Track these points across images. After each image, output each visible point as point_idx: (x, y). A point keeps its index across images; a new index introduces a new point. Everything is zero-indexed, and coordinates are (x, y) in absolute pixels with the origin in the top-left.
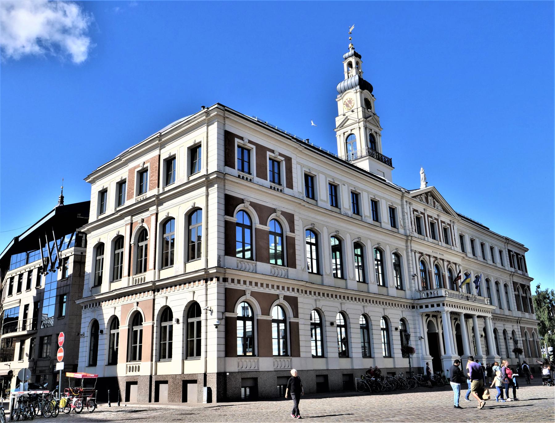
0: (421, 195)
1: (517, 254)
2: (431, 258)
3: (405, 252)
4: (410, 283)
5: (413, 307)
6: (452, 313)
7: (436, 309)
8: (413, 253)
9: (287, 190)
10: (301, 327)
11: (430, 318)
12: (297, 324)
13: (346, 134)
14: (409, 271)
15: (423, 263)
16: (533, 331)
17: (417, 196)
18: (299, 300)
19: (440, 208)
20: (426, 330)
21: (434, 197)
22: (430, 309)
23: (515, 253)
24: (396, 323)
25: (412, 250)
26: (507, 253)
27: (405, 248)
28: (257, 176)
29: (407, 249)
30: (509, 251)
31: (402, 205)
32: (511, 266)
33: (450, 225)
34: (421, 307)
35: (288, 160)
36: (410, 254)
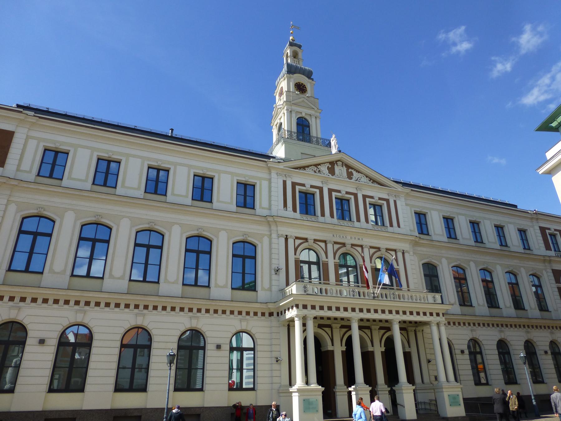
0: (319, 164)
2: (330, 246)
3: (266, 240)
4: (271, 280)
5: (271, 314)
8: (283, 240)
14: (271, 264)
17: (308, 166)
19: (364, 179)
25: (279, 236)
26: (539, 231)
27: (268, 233)
29: (270, 236)
30: (543, 230)
31: (270, 181)
33: (388, 201)
36: (274, 241)
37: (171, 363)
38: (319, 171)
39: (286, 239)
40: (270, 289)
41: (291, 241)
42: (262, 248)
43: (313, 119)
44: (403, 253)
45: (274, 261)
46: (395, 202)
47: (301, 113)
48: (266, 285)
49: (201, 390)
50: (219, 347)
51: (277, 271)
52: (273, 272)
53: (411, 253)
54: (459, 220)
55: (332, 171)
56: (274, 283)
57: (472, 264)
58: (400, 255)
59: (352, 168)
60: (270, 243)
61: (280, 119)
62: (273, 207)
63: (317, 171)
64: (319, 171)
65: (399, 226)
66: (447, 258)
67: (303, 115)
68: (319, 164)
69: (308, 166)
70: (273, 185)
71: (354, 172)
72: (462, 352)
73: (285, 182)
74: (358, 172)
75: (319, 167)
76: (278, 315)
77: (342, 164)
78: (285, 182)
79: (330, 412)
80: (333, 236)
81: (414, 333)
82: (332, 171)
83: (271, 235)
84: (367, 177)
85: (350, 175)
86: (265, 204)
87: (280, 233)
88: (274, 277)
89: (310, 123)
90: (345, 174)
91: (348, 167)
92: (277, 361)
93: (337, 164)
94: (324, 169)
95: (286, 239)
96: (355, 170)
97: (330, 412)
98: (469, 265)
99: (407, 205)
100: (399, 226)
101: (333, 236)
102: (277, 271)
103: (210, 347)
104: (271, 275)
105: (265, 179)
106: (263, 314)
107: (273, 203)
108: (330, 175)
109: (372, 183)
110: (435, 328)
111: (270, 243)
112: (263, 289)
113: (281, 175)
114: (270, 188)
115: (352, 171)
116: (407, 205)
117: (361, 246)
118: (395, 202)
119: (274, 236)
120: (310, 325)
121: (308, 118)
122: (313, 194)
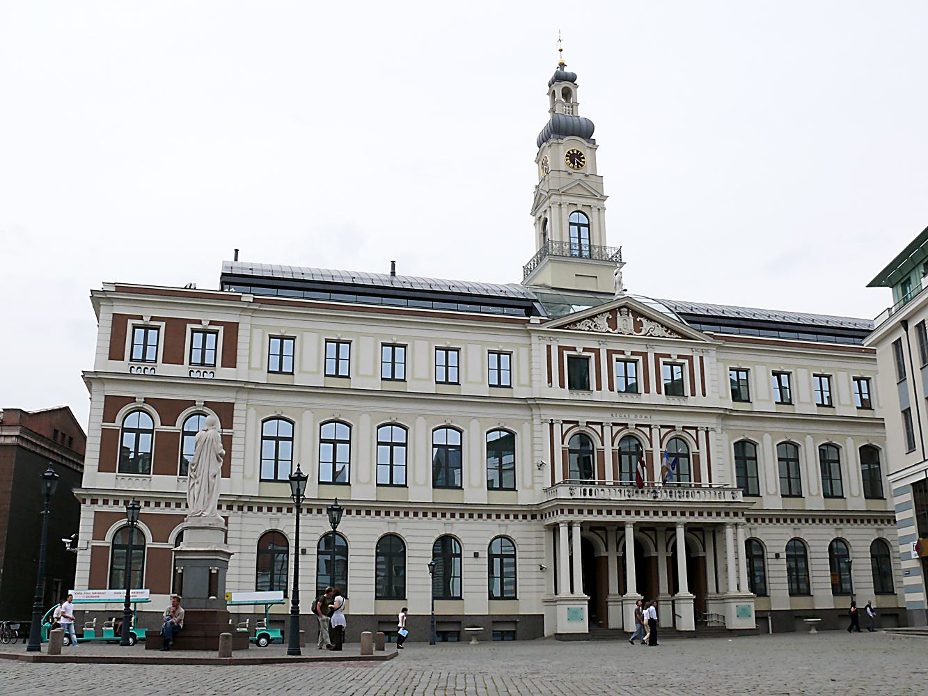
0: (596, 316)
2: (607, 430)
3: (526, 426)
5: (534, 517)
9: (223, 373)
13: (542, 220)
14: (533, 457)
17: (580, 321)
19: (660, 331)
35: (232, 330)
36: (536, 428)
38: (595, 326)
39: (552, 425)
40: (532, 487)
41: (557, 427)
42: (522, 437)
43: (595, 213)
44: (707, 432)
45: (536, 454)
46: (701, 358)
47: (576, 204)
48: (528, 483)
49: (460, 598)
50: (476, 555)
51: (541, 466)
52: (537, 468)
53: (719, 430)
54: (796, 377)
55: (613, 323)
56: (537, 480)
57: (809, 439)
58: (702, 434)
59: (642, 316)
60: (532, 431)
61: (545, 211)
62: (534, 384)
63: (592, 327)
64: (595, 326)
65: (704, 395)
66: (771, 433)
68: (596, 316)
69: (580, 321)
70: (534, 353)
72: (777, 556)
73: (549, 347)
74: (650, 319)
75: (595, 319)
76: (542, 518)
77: (628, 312)
78: (549, 347)
79: (601, 622)
80: (612, 415)
81: (712, 533)
82: (613, 323)
83: (532, 420)
84: (662, 326)
85: (638, 326)
86: (524, 379)
87: (543, 418)
88: (538, 473)
89: (591, 221)
91: (636, 314)
92: (541, 569)
93: (620, 312)
94: (602, 323)
95: (552, 425)
96: (646, 317)
97: (601, 622)
98: (804, 441)
99: (718, 360)
100: (704, 395)
101: (612, 415)
102: (541, 466)
103: (467, 554)
104: (533, 470)
105: (523, 346)
106: (525, 517)
107: (534, 378)
108: (610, 330)
109: (670, 334)
110: (729, 531)
111: (532, 431)
112: (523, 487)
113: (543, 338)
114: (530, 356)
115: (642, 319)
116: (718, 360)
117: (649, 426)
118: (701, 358)
119: (536, 421)
120: (577, 531)
122: (588, 358)
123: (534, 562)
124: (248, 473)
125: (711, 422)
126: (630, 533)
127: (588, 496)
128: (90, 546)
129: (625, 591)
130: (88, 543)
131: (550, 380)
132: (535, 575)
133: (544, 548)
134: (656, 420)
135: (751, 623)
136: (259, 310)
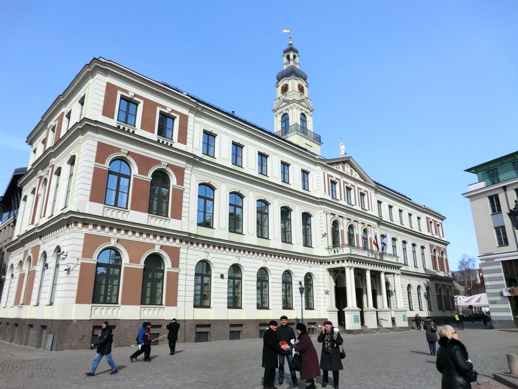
1: (435, 222)
6: (356, 269)
7: (341, 265)
10: (180, 277)
11: (340, 274)
12: (177, 274)
13: (282, 114)
15: (335, 224)
16: (448, 287)
18: (181, 250)
19: (358, 177)
20: (333, 284)
21: (352, 166)
22: (336, 265)
23: (433, 220)
24: (298, 278)
28: (142, 128)
30: (427, 218)
32: (429, 231)
34: (329, 263)
35: (184, 119)
37: (301, 292)
55: (344, 169)
58: (372, 229)
67: (304, 112)
71: (353, 170)
90: (349, 172)
102: (324, 235)
121: (306, 114)
123: (322, 288)
124: (191, 220)
125: (375, 224)
126: (368, 274)
127: (336, 254)
128: (79, 262)
129: (345, 305)
130: (78, 260)
131: (325, 191)
132: (322, 296)
133: (326, 281)
134: (360, 219)
135: (406, 324)
136: (201, 113)
